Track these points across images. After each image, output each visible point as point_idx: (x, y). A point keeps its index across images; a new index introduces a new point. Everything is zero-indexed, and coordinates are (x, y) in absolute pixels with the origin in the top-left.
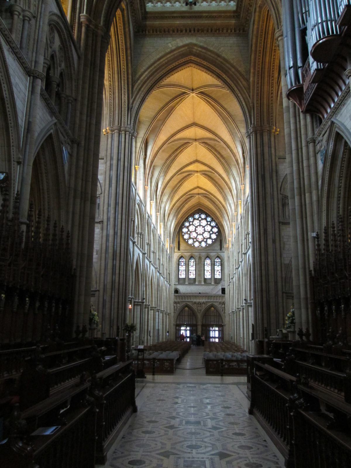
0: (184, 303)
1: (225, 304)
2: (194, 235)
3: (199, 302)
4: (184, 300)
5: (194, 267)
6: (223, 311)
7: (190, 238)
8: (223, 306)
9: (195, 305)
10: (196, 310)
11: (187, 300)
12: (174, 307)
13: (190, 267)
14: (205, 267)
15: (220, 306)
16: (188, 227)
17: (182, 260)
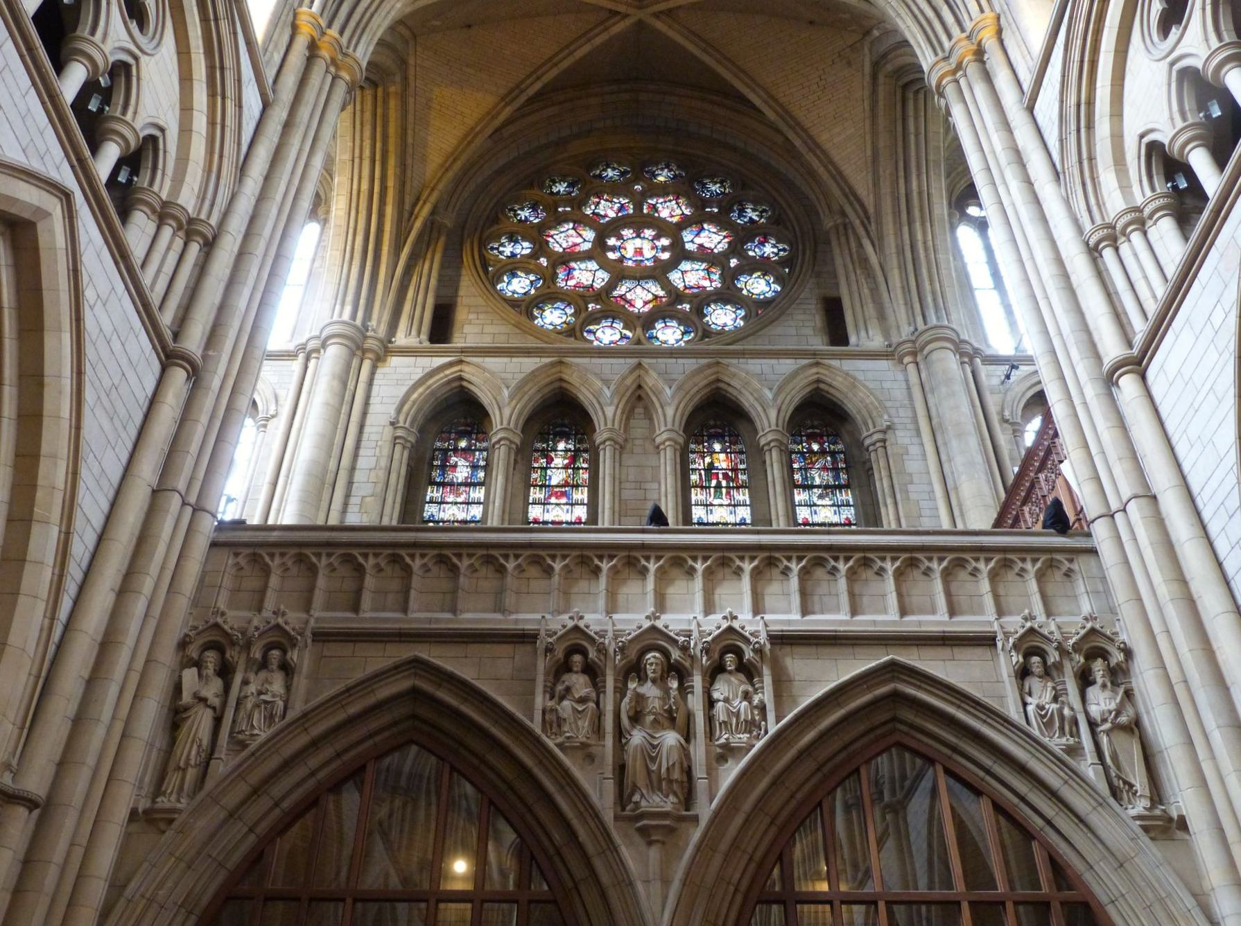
0: (378, 658)
1: (1118, 675)
2: (587, 275)
3: (654, 638)
4: (371, 615)
5: (582, 495)
6: (1119, 790)
7: (548, 295)
8: (1101, 701)
9: (579, 683)
10: (603, 795)
11: (420, 615)
12: (176, 717)
13: (535, 494)
14: (696, 496)
15: (1041, 694)
16: (538, 237)
17: (463, 444)
